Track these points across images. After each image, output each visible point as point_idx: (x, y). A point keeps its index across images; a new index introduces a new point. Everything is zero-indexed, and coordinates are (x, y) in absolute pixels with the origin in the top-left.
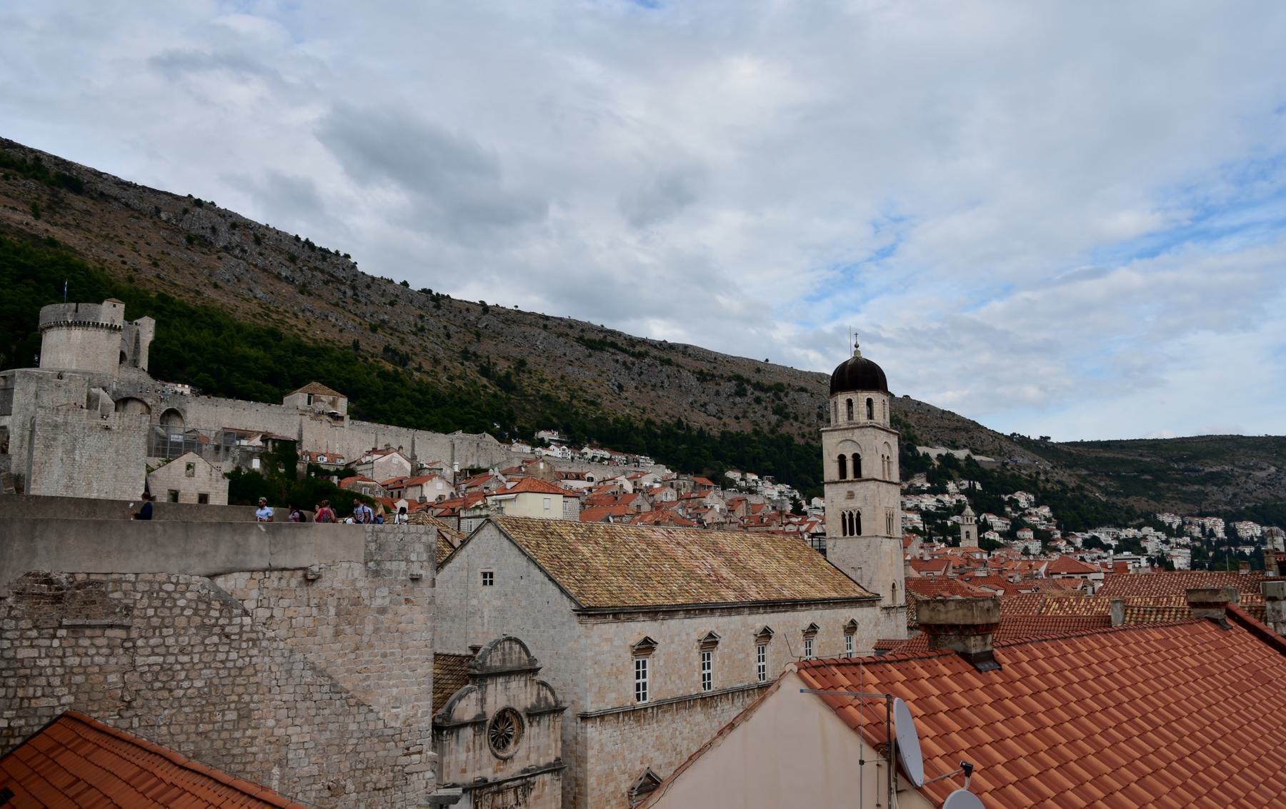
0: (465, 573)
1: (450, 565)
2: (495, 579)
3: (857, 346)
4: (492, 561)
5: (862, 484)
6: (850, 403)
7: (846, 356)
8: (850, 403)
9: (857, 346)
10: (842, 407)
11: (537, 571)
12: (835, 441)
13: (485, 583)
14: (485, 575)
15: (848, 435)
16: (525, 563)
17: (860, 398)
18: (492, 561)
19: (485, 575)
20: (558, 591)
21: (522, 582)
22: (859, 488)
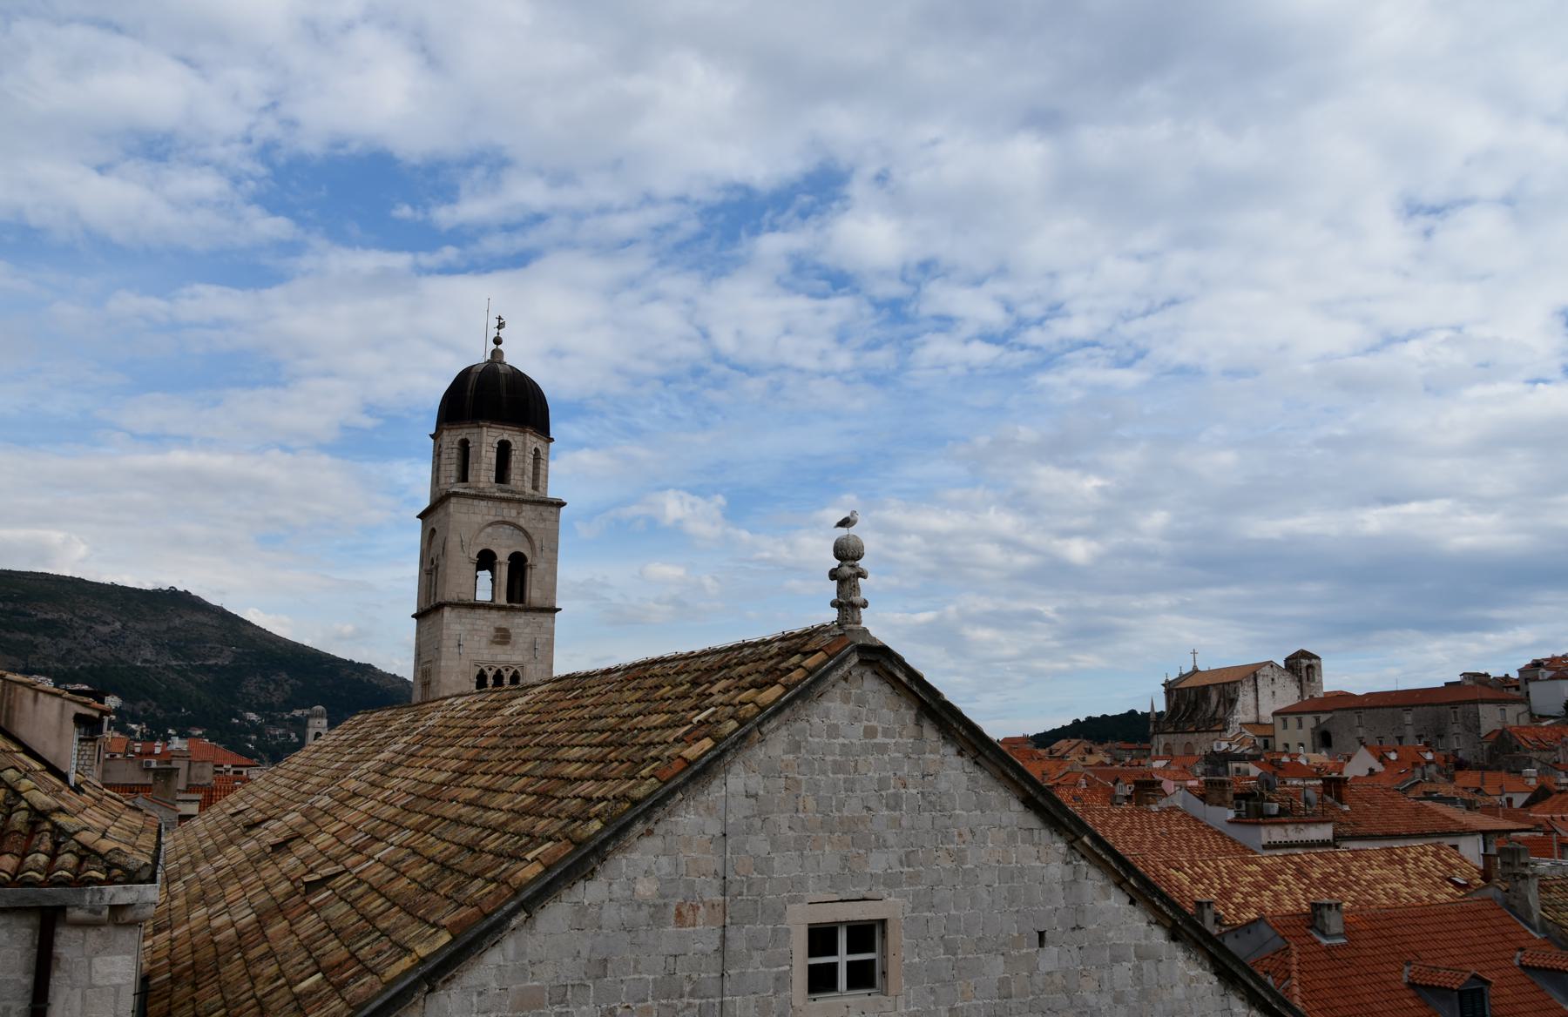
0: (703, 936)
1: (590, 892)
2: (901, 953)
3: (497, 341)
4: (878, 863)
5: (529, 617)
6: (504, 450)
7: (478, 355)
8: (504, 450)
9: (497, 341)
10: (489, 456)
11: (1117, 901)
12: (478, 519)
13: (821, 981)
14: (822, 939)
15: (510, 513)
16: (1056, 870)
17: (523, 443)
18: (878, 863)
19: (822, 939)
20: (1206, 981)
21: (1049, 959)
22: (520, 625)
